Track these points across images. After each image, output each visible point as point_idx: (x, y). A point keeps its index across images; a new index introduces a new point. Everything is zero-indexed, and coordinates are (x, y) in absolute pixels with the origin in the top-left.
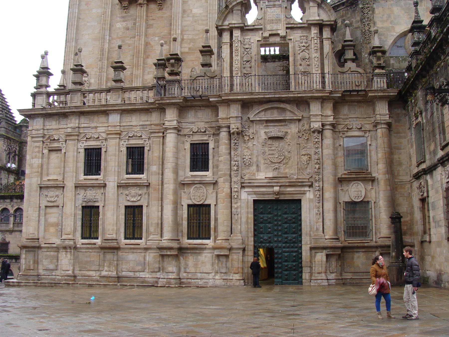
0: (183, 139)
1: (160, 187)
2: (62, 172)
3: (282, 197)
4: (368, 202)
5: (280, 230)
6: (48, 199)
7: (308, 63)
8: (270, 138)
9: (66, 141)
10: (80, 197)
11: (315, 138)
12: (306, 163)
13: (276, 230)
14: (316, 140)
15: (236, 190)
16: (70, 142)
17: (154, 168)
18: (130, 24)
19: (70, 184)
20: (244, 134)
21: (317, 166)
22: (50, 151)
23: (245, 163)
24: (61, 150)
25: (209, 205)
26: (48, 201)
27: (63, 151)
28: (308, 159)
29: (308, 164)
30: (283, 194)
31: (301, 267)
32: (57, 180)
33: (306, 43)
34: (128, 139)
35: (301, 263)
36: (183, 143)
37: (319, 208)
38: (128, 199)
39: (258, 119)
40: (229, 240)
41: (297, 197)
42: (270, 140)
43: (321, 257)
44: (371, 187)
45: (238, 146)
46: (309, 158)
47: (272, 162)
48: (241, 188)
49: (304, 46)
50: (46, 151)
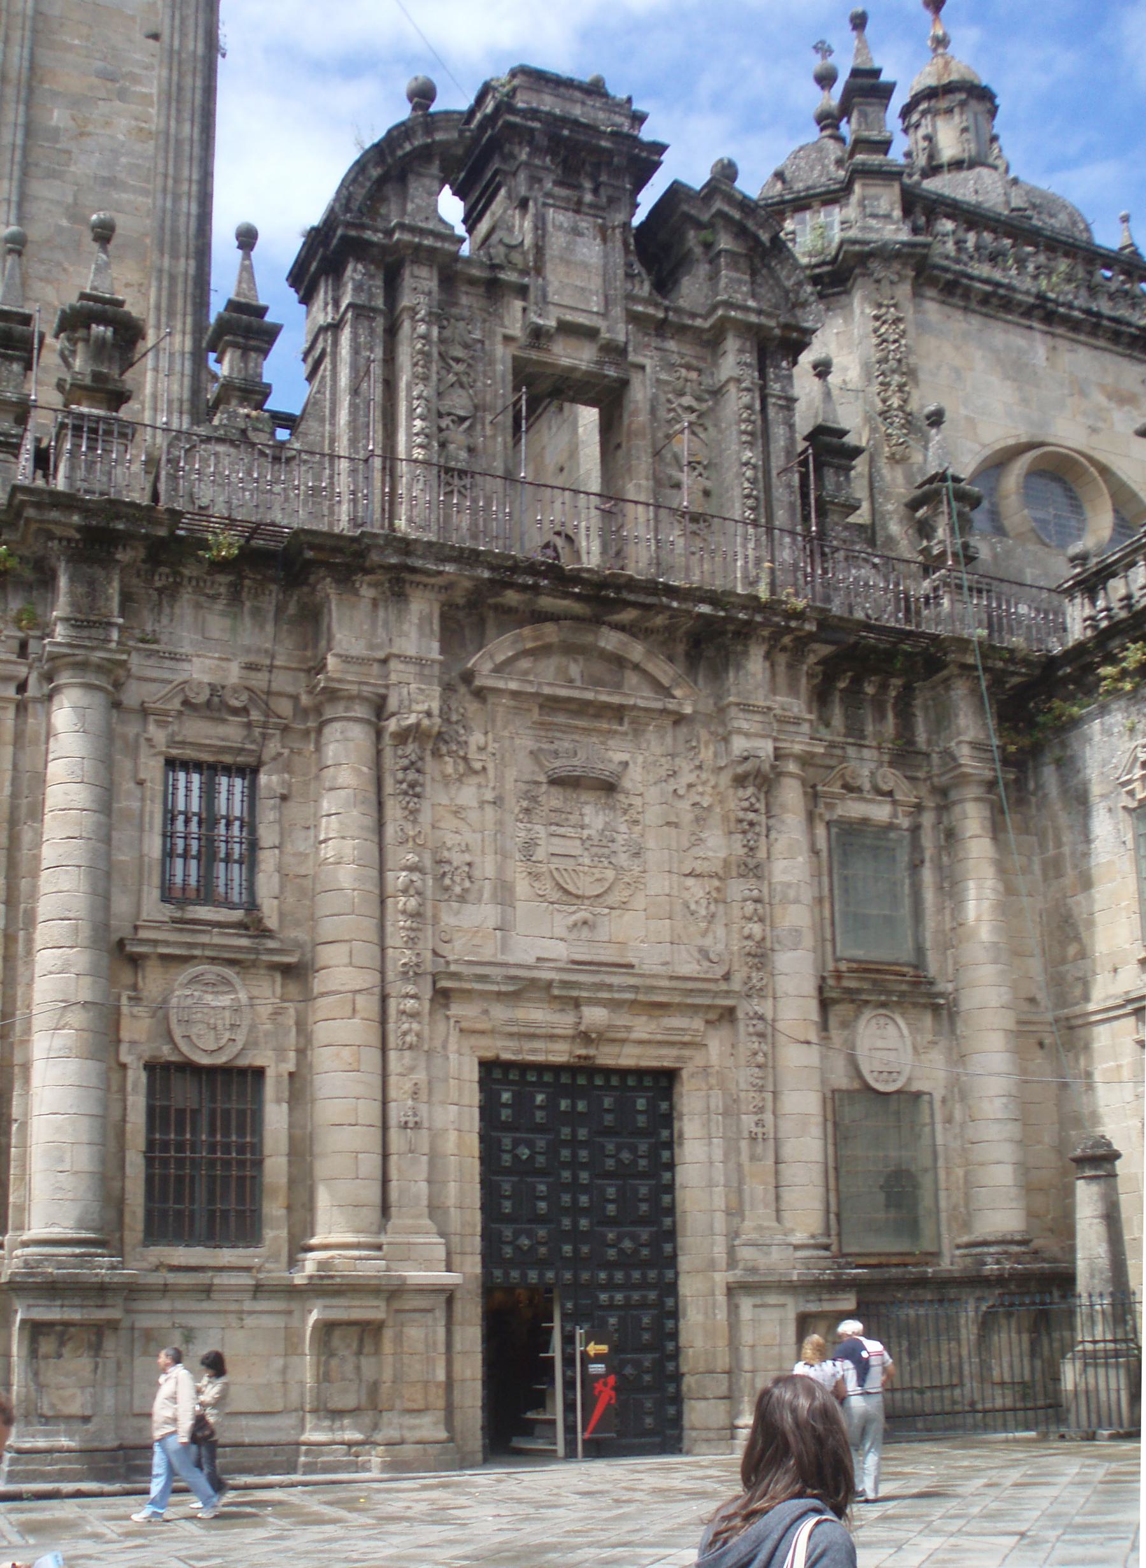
0: (132, 729)
3: (607, 1056)
4: (918, 1095)
5: (585, 1212)
7: (708, 484)
8: (554, 782)
11: (746, 804)
12: (703, 912)
13: (566, 1211)
14: (751, 816)
15: (410, 1004)
20: (444, 749)
21: (756, 929)
23: (447, 881)
25: (259, 1073)
28: (714, 894)
29: (713, 916)
30: (613, 1041)
33: (699, 399)
35: (675, 1355)
36: (133, 751)
37: (761, 1110)
39: (513, 686)
40: (379, 1247)
41: (663, 1058)
42: (554, 790)
44: (930, 1037)
45: (418, 796)
46: (718, 889)
47: (567, 892)
48: (432, 1000)
49: (691, 410)
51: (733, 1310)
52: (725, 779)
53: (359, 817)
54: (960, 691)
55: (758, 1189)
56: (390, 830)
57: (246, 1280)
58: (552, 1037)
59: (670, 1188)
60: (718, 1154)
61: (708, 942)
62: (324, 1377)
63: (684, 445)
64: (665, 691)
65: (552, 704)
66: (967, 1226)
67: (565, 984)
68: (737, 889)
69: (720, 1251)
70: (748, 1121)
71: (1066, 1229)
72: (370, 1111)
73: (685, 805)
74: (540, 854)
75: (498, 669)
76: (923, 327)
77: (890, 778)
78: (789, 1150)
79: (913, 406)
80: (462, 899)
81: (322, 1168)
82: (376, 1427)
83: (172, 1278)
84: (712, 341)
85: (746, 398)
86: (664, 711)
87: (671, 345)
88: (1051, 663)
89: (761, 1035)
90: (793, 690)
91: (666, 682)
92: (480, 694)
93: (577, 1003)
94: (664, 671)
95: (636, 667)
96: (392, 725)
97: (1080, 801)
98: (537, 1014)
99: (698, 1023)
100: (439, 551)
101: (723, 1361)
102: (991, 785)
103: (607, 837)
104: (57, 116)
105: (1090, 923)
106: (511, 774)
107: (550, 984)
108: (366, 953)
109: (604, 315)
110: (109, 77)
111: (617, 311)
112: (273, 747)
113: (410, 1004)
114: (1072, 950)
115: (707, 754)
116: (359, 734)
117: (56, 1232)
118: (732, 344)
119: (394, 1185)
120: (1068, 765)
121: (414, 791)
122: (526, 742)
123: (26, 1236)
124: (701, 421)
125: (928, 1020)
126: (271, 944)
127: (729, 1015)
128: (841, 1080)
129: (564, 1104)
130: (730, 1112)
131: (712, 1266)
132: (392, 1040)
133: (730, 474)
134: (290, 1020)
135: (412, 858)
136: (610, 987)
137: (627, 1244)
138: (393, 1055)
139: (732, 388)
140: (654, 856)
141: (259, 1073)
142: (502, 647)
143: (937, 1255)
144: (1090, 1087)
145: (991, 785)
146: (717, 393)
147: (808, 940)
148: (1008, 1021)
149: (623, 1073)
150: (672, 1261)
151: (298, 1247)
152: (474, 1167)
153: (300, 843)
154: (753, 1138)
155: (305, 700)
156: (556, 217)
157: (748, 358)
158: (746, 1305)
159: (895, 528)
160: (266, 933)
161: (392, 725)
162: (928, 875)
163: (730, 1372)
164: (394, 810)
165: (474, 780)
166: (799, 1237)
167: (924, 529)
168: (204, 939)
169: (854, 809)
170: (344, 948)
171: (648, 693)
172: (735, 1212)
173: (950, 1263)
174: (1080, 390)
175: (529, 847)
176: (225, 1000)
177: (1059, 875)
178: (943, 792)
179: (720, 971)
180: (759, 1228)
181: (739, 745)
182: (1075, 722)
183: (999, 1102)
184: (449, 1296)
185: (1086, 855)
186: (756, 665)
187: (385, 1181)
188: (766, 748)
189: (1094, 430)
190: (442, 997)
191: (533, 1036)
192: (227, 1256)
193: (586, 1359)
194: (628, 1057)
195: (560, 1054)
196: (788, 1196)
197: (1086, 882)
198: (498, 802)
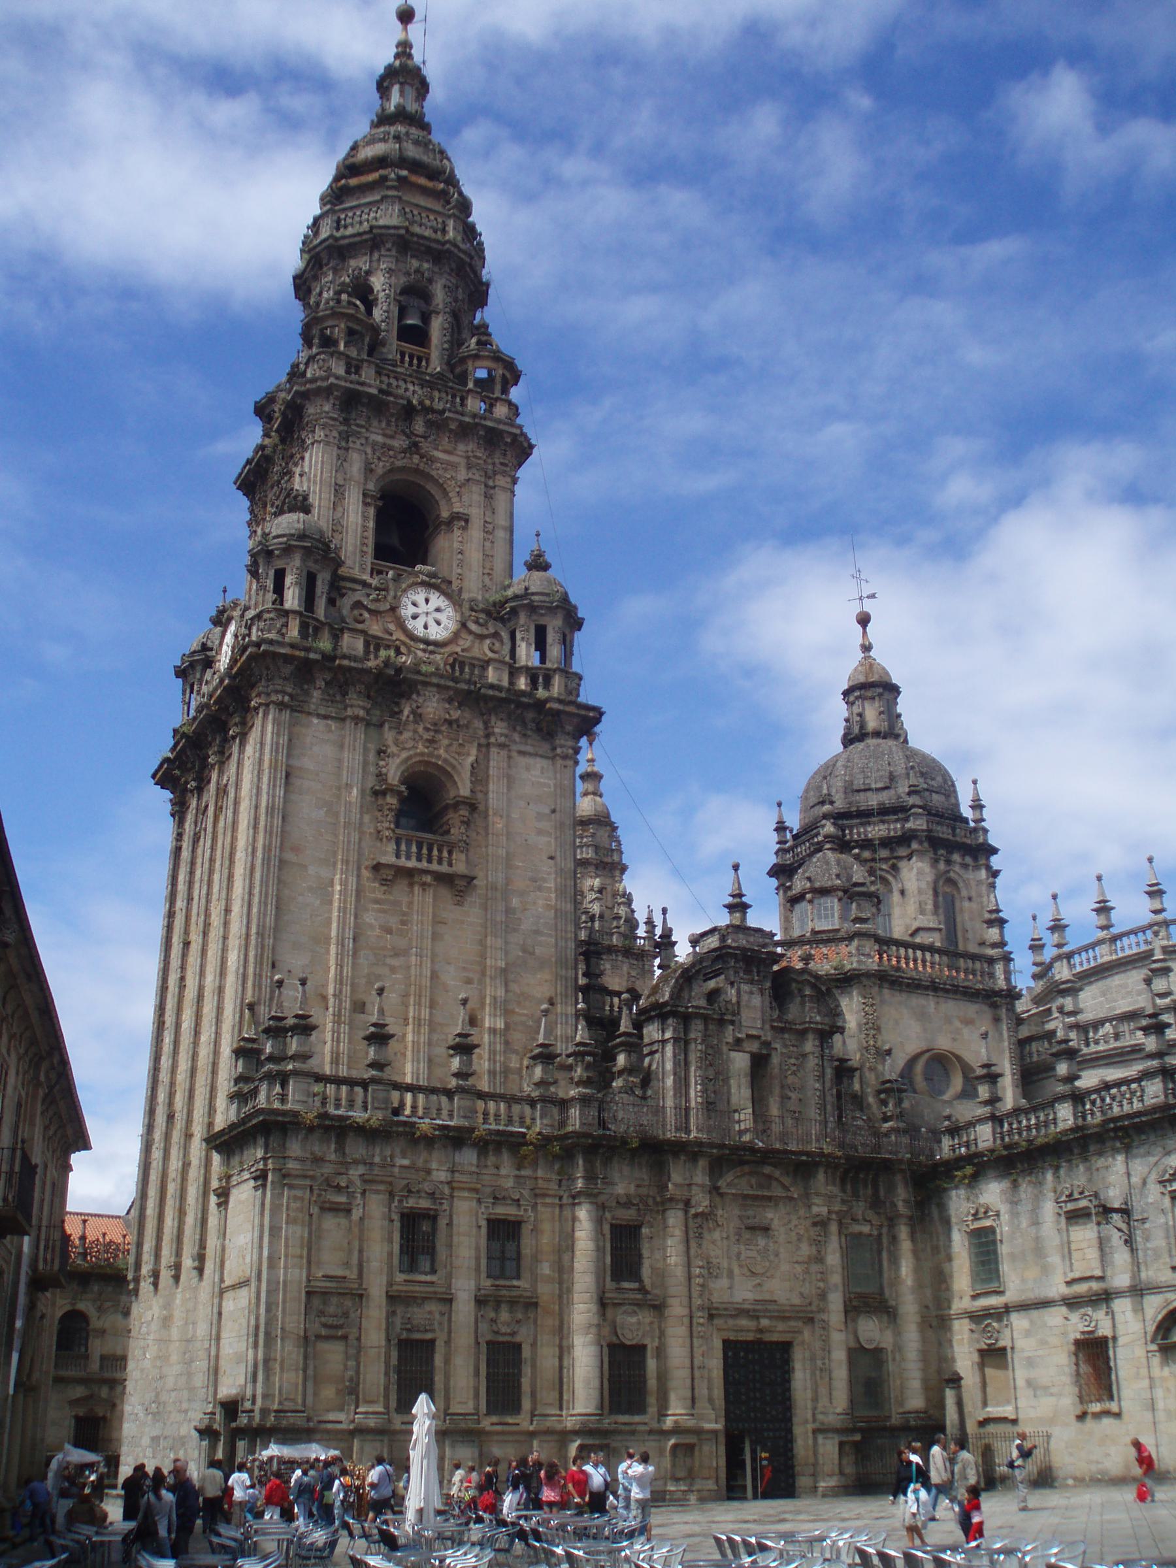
1: (557, 1307)
2: (355, 1260)
3: (768, 1337)
6: (323, 1319)
7: (800, 1096)
8: (749, 1228)
9: (364, 1193)
10: (398, 1321)
15: (702, 1320)
16: (374, 1196)
17: (546, 1269)
18: (393, 922)
19: (377, 1288)
21: (821, 1285)
22: (322, 1209)
24: (348, 1211)
25: (644, 1347)
26: (325, 1326)
27: (356, 1214)
31: (792, 1467)
32: (345, 1278)
33: (797, 1059)
34: (493, 1204)
35: (792, 1458)
37: (824, 1359)
38: (495, 1328)
43: (829, 1448)
50: (315, 1210)
51: (815, 1439)
52: (808, 1222)
53: (681, 1248)
54: (898, 1178)
55: (823, 1391)
56: (692, 1252)
57: (646, 1428)
58: (748, 1331)
59: (789, 1390)
60: (808, 1376)
61: (803, 1290)
62: (674, 1465)
63: (791, 1079)
64: (787, 1189)
65: (745, 1197)
66: (901, 1404)
67: (754, 1310)
68: (815, 1268)
69: (809, 1416)
70: (819, 1363)
71: (941, 1406)
72: (687, 1362)
73: (793, 1234)
74: (743, 1257)
75: (728, 1185)
76: (883, 1002)
77: (870, 1214)
78: (835, 1374)
79: (879, 1044)
80: (716, 1277)
81: (672, 1384)
82: (691, 1485)
83: (623, 1427)
84: (802, 1033)
85: (816, 1061)
86: (787, 1197)
87: (786, 1036)
88: (936, 1165)
89: (824, 1328)
90: (834, 1184)
91: (787, 1184)
92: (721, 1195)
93: (758, 1318)
94: (786, 1181)
95: (776, 1179)
96: (693, 1211)
97: (947, 1223)
98: (744, 1322)
99: (800, 1324)
100: (711, 1145)
101: (811, 1460)
102: (911, 1218)
103: (766, 1250)
104: (515, 902)
105: (951, 1277)
106: (732, 1225)
107: (748, 1311)
108: (685, 1301)
109: (762, 1029)
110: (534, 880)
111: (767, 1027)
112: (648, 1218)
113: (702, 1320)
114: (944, 1286)
115: (802, 1212)
116: (680, 1214)
117: (589, 1411)
118: (811, 1036)
119: (696, 1391)
120: (942, 1207)
121: (700, 1236)
122: (737, 1212)
123: (575, 1412)
124: (800, 1067)
125: (885, 1318)
126: (649, 1297)
127: (811, 1320)
128: (853, 1344)
129: (750, 1356)
130: (813, 1359)
131: (806, 1422)
132: (695, 1334)
133: (810, 1093)
134: (656, 1326)
135: (701, 1264)
136: (770, 1311)
137: (774, 1413)
138: (695, 1340)
139: (811, 1057)
140: (783, 1254)
141: (644, 1347)
142: (729, 1177)
143: (889, 1417)
144: (952, 1346)
145: (911, 1218)
146: (804, 1056)
147: (841, 1288)
148: (917, 1318)
149: (772, 1343)
150: (790, 1420)
151: (662, 1414)
152: (722, 1381)
153: (658, 1255)
154: (821, 1370)
155: (658, 1199)
156: (745, 987)
157: (817, 1043)
158: (820, 1439)
159: (871, 1100)
160: (647, 1292)
161: (693, 1211)
162: (885, 1255)
163: (815, 1465)
164: (693, 1244)
165: (719, 1229)
166: (839, 1410)
167: (884, 1103)
168: (626, 1296)
169: (856, 1228)
170: (678, 1300)
171: (780, 1189)
172: (815, 1399)
173: (895, 1420)
174: (948, 1020)
175: (739, 1254)
176: (634, 1320)
177: (938, 1253)
178: (891, 1219)
179: (807, 1301)
180: (824, 1407)
181: (815, 1210)
182: (945, 1190)
183: (915, 1353)
184: (715, 1432)
185: (949, 1247)
186: (821, 1176)
187: (693, 1389)
188: (824, 1210)
189: (954, 1040)
190: (711, 1317)
191: (742, 1331)
192: (637, 1419)
193: (761, 1459)
194: (775, 1337)
195: (750, 1337)
196: (835, 1393)
197: (949, 1259)
198: (728, 1238)
